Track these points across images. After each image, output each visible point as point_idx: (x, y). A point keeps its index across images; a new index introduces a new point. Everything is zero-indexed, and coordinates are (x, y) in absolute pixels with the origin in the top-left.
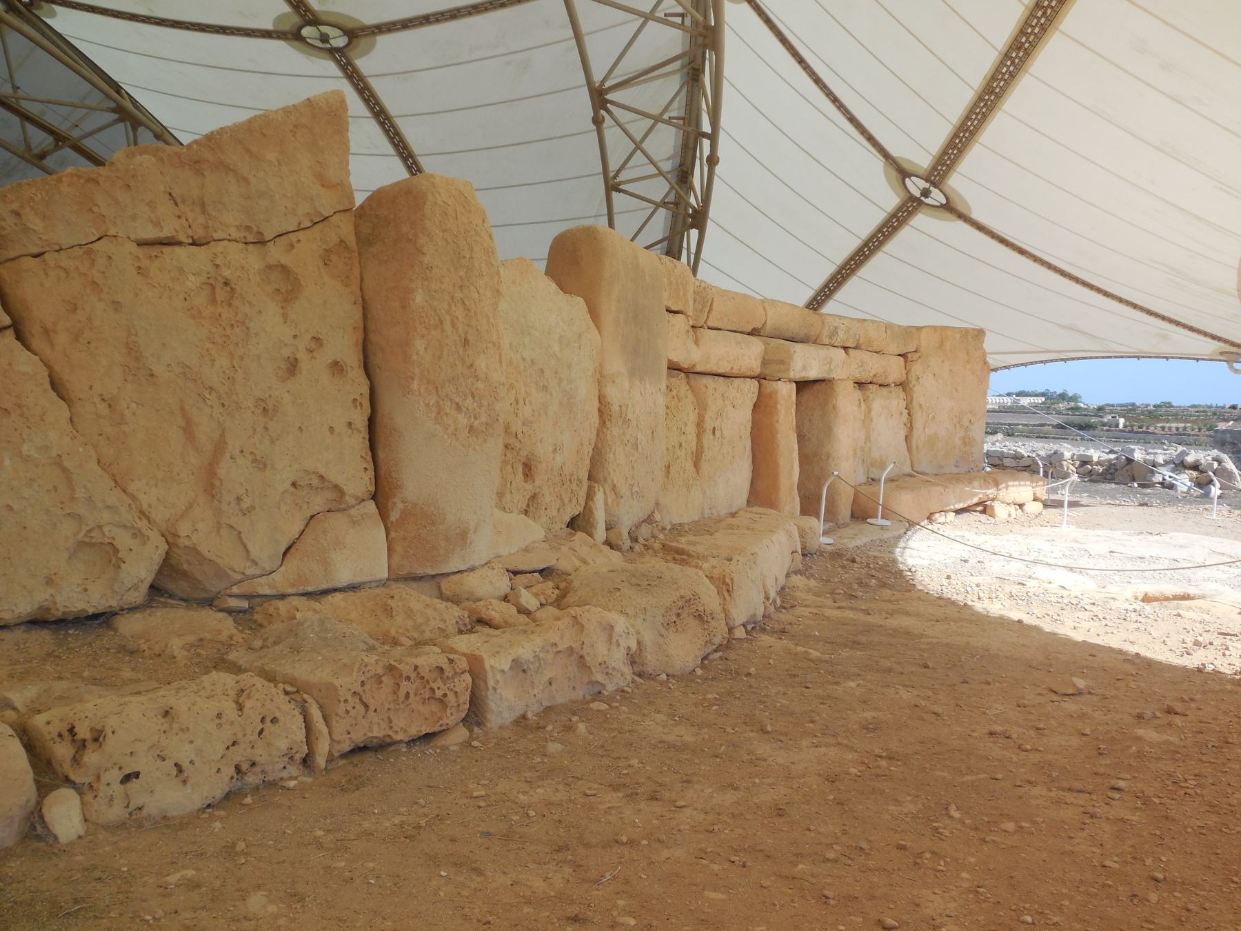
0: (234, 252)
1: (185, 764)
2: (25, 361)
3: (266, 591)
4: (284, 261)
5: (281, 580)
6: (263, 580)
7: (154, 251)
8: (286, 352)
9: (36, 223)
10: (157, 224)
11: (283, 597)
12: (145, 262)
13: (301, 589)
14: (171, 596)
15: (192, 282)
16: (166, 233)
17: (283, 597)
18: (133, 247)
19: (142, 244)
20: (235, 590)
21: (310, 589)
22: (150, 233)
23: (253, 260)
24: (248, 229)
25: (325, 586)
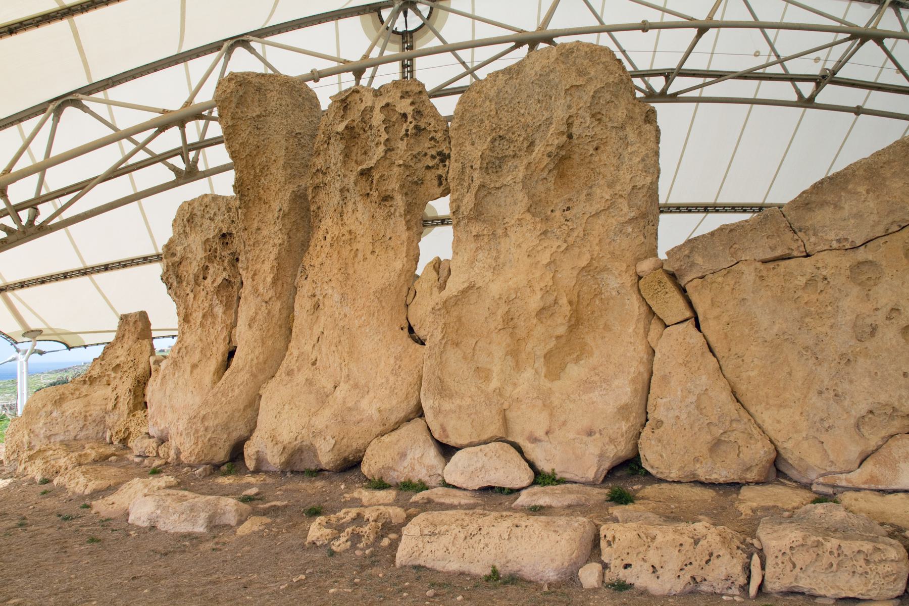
0: (830, 259)
1: (657, 566)
2: (695, 338)
3: (844, 484)
4: (870, 258)
5: (858, 477)
6: (844, 476)
7: (771, 265)
8: (869, 321)
9: (699, 260)
10: (773, 249)
11: (858, 490)
12: (764, 273)
13: (873, 486)
14: (790, 479)
15: (802, 281)
16: (778, 253)
17: (858, 490)
18: (759, 265)
19: (764, 262)
20: (821, 480)
21: (880, 487)
22: (770, 255)
23: (847, 261)
24: (846, 239)
25: (895, 487)
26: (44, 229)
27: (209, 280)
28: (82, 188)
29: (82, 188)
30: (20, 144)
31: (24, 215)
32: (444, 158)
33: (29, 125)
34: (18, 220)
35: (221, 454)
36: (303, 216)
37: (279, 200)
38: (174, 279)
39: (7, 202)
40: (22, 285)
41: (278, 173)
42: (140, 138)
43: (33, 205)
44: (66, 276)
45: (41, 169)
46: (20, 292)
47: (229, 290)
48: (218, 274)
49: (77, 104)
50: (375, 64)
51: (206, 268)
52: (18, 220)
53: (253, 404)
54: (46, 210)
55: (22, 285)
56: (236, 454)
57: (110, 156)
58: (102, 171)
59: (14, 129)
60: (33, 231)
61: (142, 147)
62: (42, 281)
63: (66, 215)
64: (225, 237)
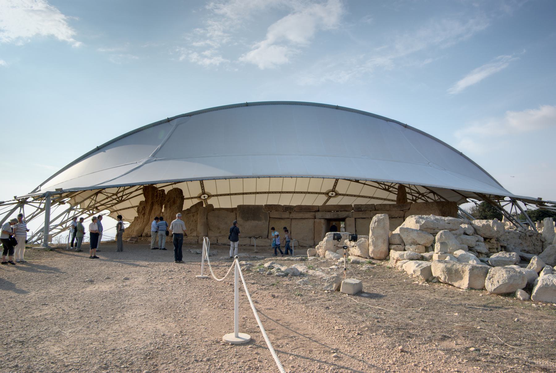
26: (124, 200)
31: (120, 198)
35: (140, 235)
36: (152, 204)
37: (150, 203)
38: (138, 211)
40: (120, 210)
41: (150, 199)
43: (122, 196)
44: (129, 208)
45: (123, 191)
47: (144, 214)
48: (143, 212)
53: (144, 229)
54: (124, 197)
55: (120, 210)
56: (141, 236)
60: (122, 201)
62: (124, 209)
63: (129, 197)
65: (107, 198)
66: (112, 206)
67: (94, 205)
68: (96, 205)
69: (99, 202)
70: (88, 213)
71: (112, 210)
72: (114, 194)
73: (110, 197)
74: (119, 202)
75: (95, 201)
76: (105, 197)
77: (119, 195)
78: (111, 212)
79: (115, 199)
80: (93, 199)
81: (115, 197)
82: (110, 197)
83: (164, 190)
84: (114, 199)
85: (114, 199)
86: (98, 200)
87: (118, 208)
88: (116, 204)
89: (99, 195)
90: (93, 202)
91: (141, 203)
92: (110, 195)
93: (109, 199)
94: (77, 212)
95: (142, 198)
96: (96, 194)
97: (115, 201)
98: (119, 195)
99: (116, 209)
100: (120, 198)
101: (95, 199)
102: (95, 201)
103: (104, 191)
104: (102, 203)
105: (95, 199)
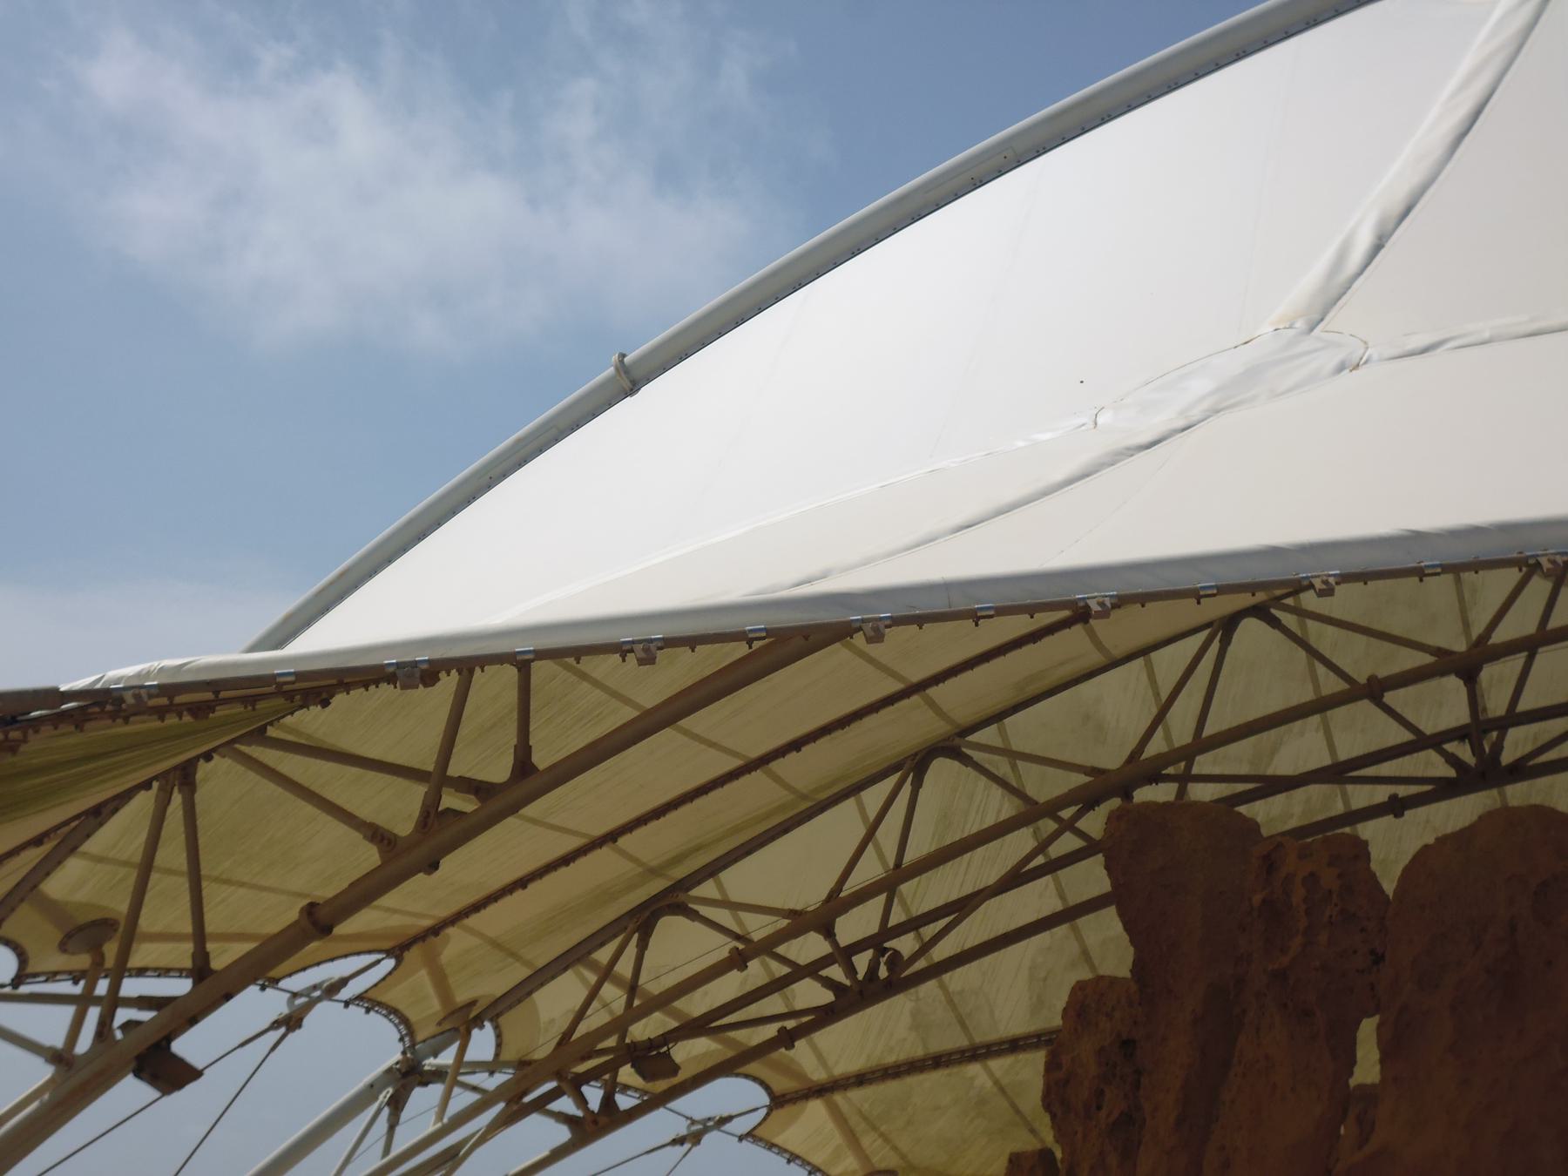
27: (1103, 1113)
28: (962, 907)
29: (962, 907)
30: (861, 832)
31: (862, 961)
32: (1378, 959)
33: (874, 797)
34: (851, 970)
39: (835, 943)
42: (1066, 814)
43: (875, 942)
45: (888, 886)
46: (855, 1094)
49: (955, 753)
50: (1529, 646)
51: (1101, 1093)
52: (851, 970)
57: (1020, 843)
58: (991, 877)
59: (849, 804)
61: (1069, 826)
63: (941, 952)
64: (1127, 1045)
65: (738, 960)
66: (787, 1039)
67: (619, 1025)
68: (642, 1031)
69: (664, 1001)
70: (566, 1104)
71: (782, 1084)
72: (799, 922)
73: (767, 947)
74: (852, 999)
75: (633, 988)
76: (721, 947)
77: (855, 925)
78: (778, 1101)
79: (812, 970)
80: (607, 974)
81: (811, 947)
82: (767, 947)
83: (1360, 849)
84: (799, 972)
85: (799, 972)
86: (655, 982)
87: (845, 1066)
88: (825, 1016)
89: (670, 928)
90: (613, 995)
91: (1088, 1001)
92: (759, 927)
93: (757, 972)
94: (462, 1100)
95: (1108, 944)
96: (641, 922)
97: (810, 994)
98: (855, 925)
99: (818, 1075)
100: (862, 961)
101: (625, 967)
102: (633, 988)
103: (707, 889)
104: (697, 1004)
105: (625, 967)
